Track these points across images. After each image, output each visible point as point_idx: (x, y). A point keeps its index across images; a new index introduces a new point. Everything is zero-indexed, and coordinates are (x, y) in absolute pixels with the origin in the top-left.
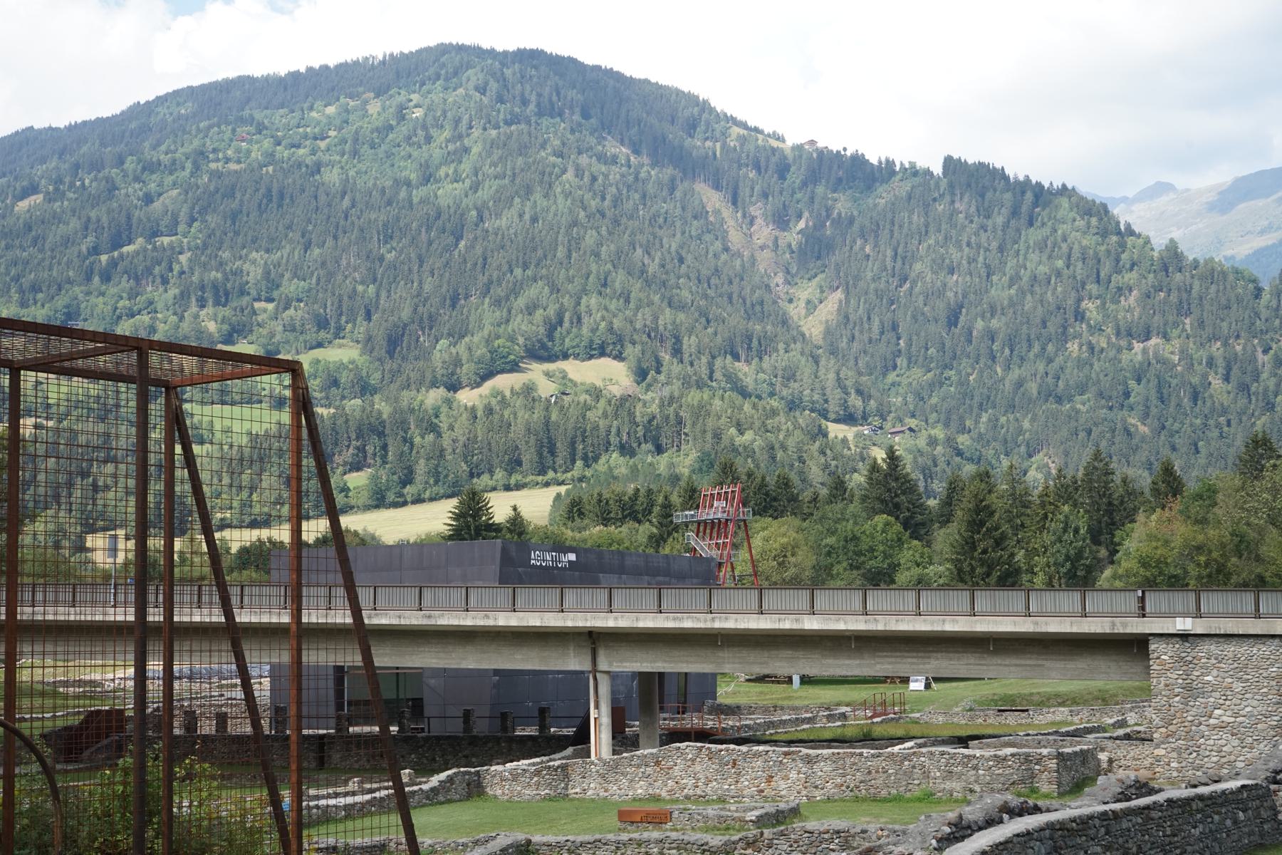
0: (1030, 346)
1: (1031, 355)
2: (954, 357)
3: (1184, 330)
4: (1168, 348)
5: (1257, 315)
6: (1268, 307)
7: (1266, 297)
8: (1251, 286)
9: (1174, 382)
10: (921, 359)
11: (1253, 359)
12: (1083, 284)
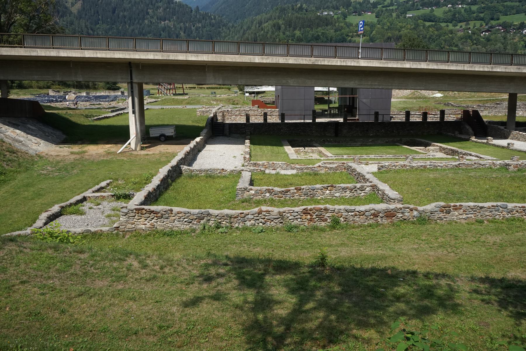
0: (135, 21)
1: (136, 23)
2: (115, 22)
3: (174, 19)
4: (170, 24)
5: (191, 17)
6: (194, 15)
7: (193, 12)
8: (190, 9)
9: (172, 32)
11: (191, 28)
12: (148, 5)
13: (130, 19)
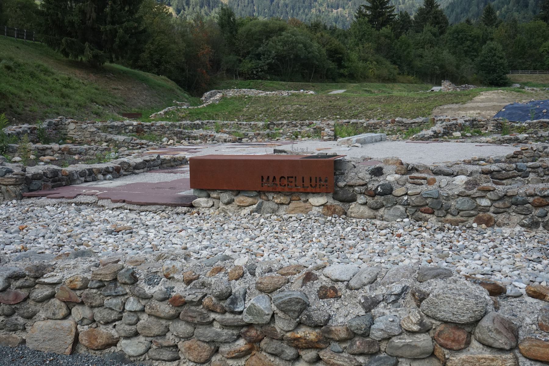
0: (300, 10)
1: (300, 12)
2: (274, 13)
10: (263, 13)
13: (293, 8)
